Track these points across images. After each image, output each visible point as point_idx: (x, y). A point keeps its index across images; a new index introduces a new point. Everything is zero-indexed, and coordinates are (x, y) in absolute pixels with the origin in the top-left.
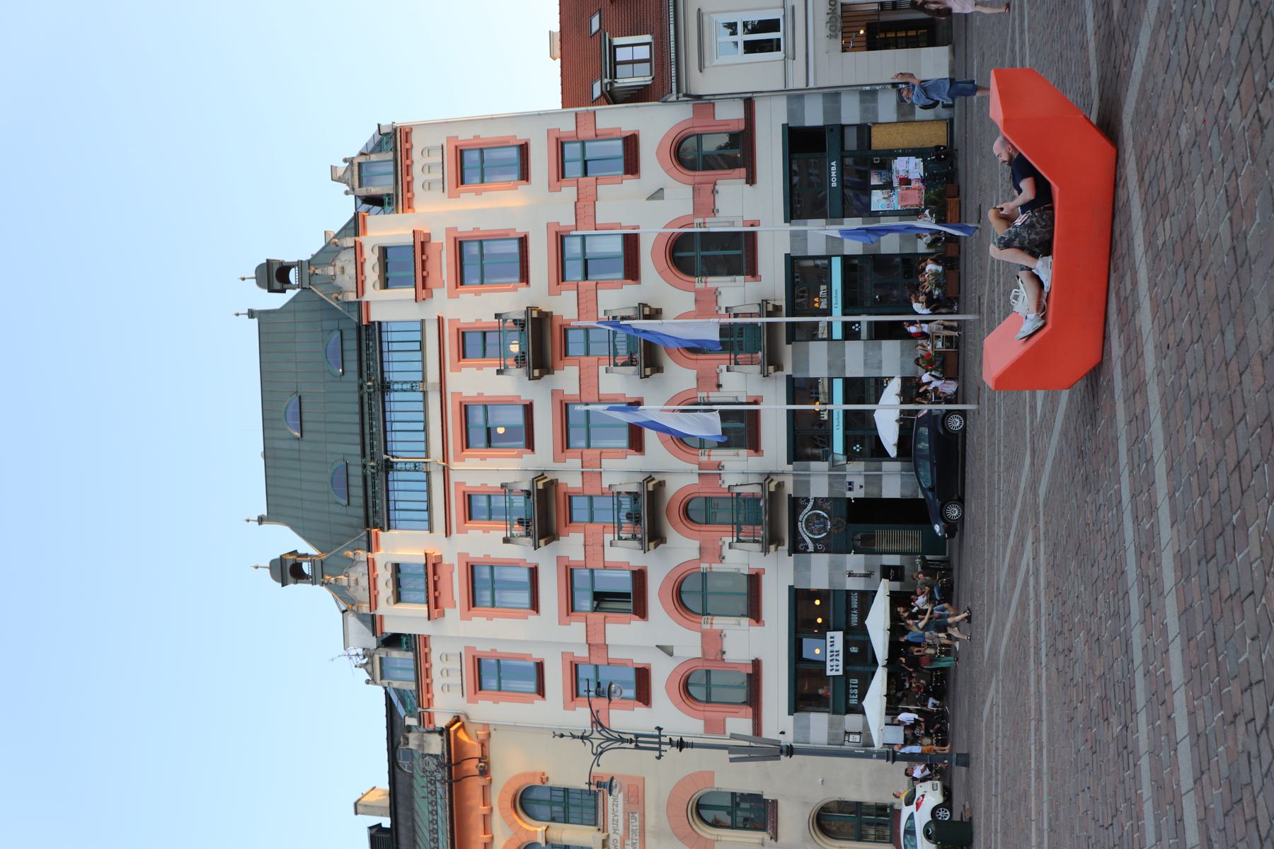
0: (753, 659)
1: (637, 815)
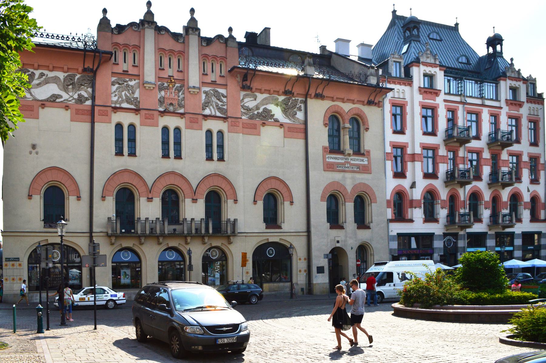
0: (414, 219)
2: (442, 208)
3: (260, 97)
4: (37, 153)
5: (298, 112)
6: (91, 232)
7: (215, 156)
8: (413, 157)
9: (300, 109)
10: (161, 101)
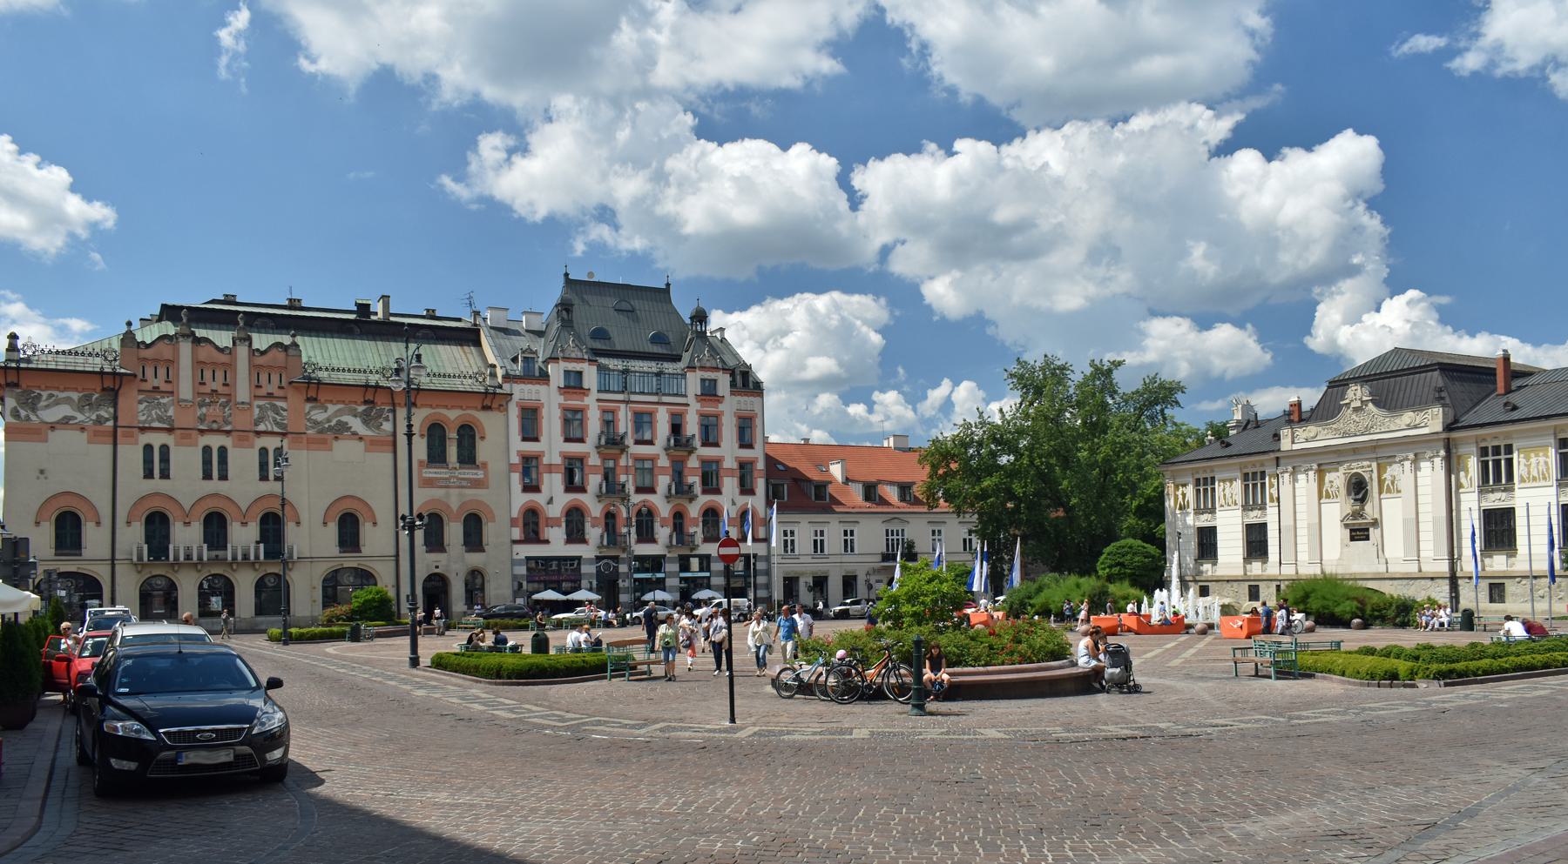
2: (593, 526)
3: (332, 408)
4: (46, 478)
5: (384, 423)
6: (113, 559)
8: (550, 468)
9: (387, 419)
10: (202, 419)
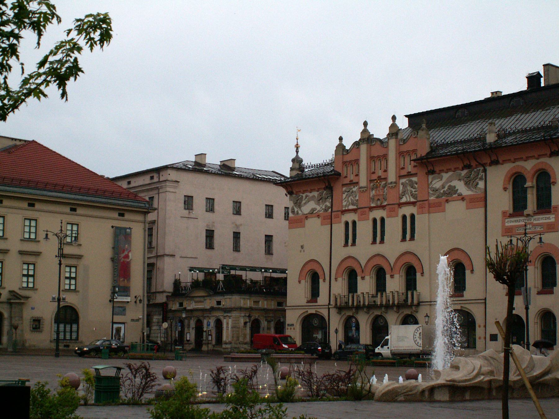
1: (542, 229)
3: (445, 176)
7: (408, 236)
9: (481, 179)
10: (372, 199)
